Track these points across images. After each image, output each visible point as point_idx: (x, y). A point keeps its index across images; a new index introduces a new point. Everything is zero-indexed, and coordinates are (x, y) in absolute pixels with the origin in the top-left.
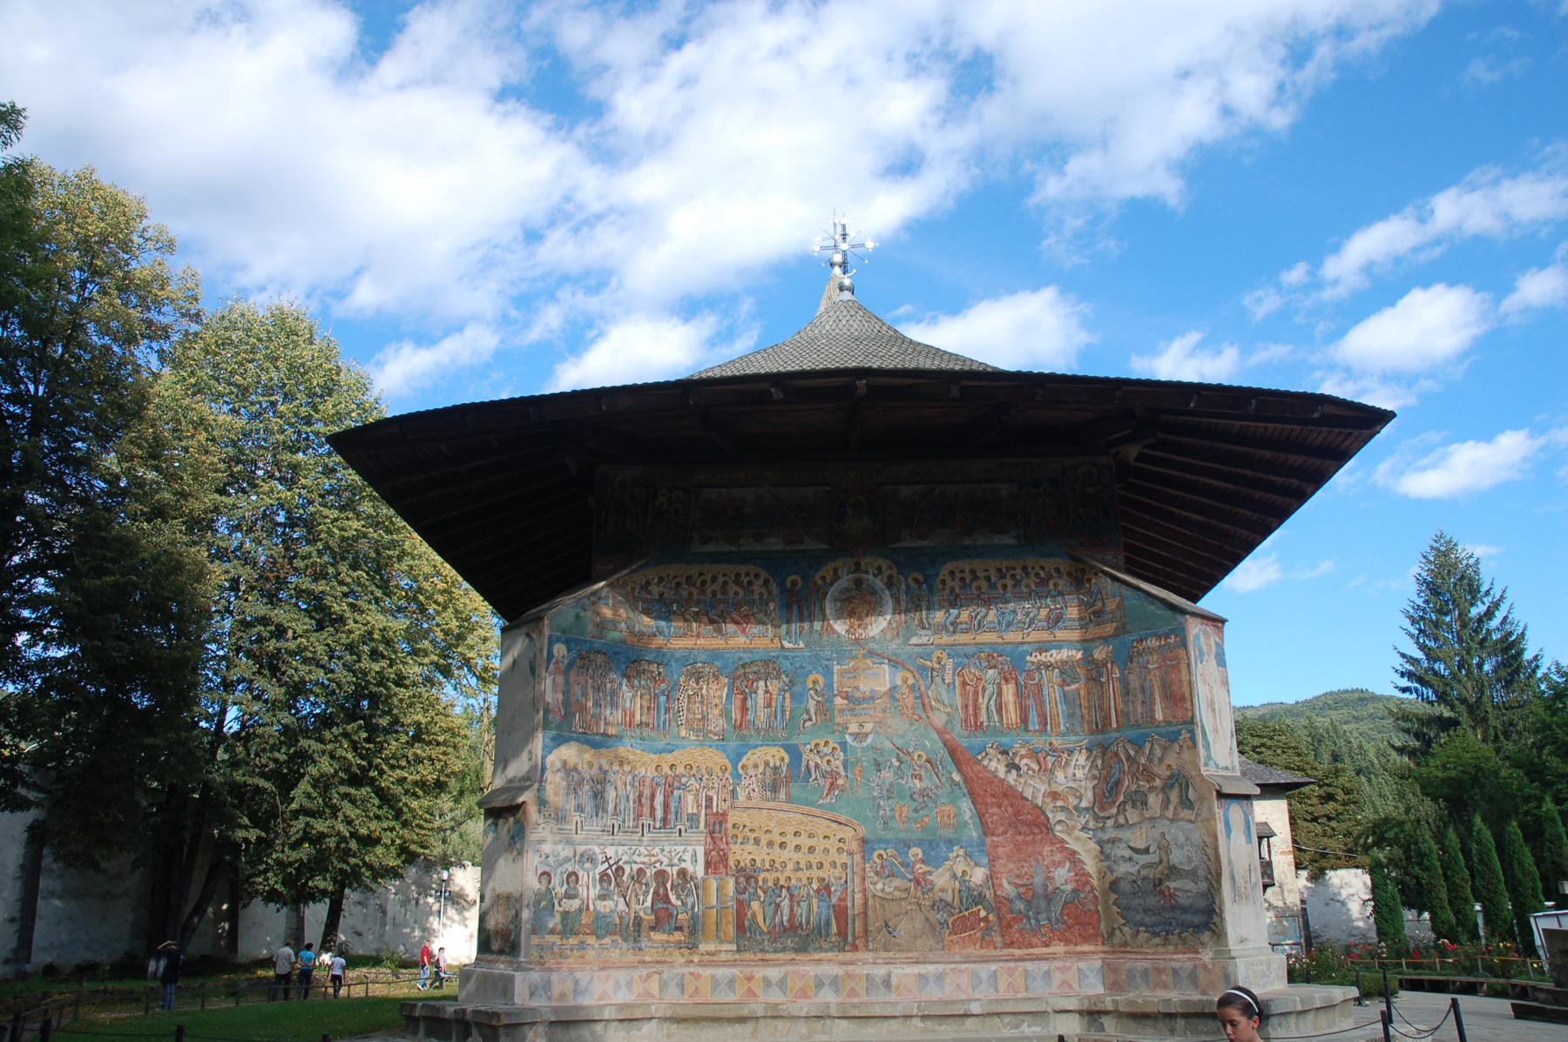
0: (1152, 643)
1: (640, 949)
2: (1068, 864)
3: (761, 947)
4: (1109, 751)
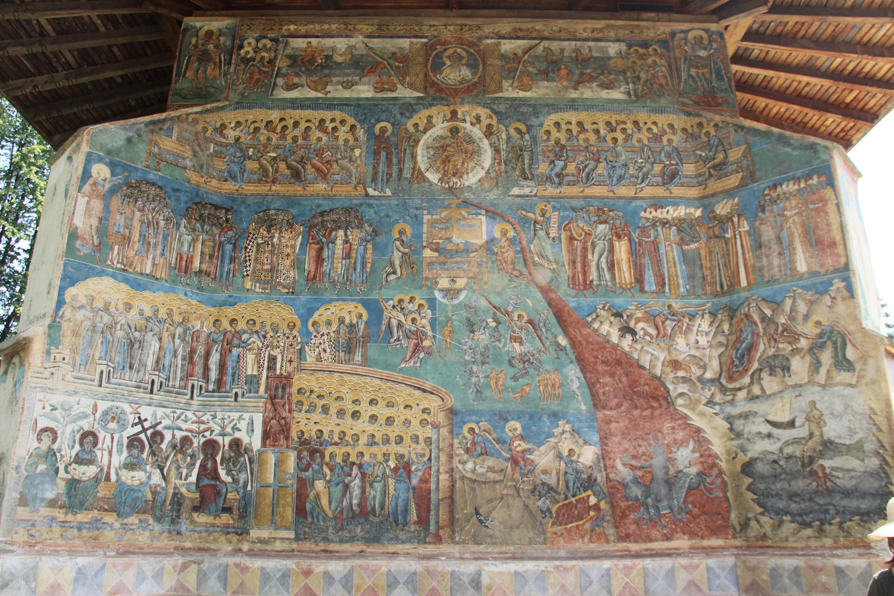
0: (791, 187)
1: (179, 533)
2: (691, 444)
3: (323, 535)
4: (738, 313)
